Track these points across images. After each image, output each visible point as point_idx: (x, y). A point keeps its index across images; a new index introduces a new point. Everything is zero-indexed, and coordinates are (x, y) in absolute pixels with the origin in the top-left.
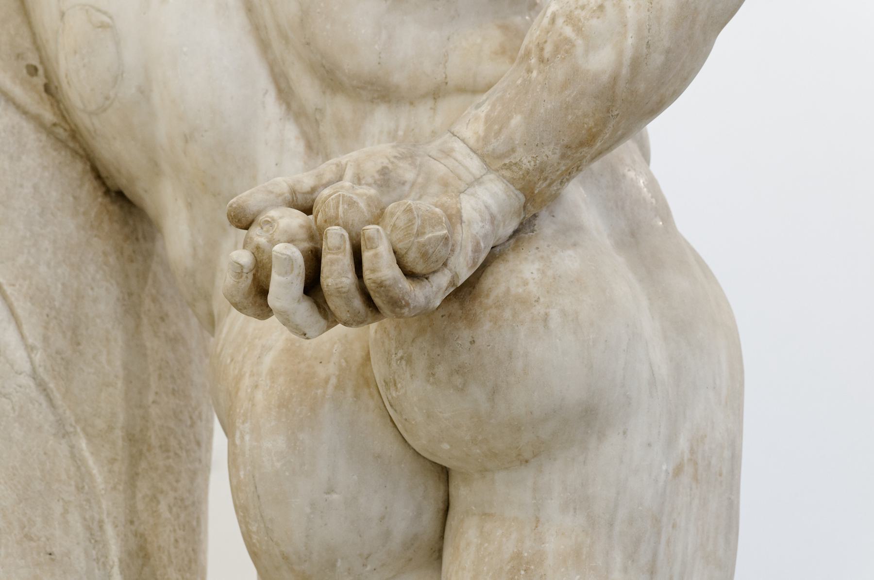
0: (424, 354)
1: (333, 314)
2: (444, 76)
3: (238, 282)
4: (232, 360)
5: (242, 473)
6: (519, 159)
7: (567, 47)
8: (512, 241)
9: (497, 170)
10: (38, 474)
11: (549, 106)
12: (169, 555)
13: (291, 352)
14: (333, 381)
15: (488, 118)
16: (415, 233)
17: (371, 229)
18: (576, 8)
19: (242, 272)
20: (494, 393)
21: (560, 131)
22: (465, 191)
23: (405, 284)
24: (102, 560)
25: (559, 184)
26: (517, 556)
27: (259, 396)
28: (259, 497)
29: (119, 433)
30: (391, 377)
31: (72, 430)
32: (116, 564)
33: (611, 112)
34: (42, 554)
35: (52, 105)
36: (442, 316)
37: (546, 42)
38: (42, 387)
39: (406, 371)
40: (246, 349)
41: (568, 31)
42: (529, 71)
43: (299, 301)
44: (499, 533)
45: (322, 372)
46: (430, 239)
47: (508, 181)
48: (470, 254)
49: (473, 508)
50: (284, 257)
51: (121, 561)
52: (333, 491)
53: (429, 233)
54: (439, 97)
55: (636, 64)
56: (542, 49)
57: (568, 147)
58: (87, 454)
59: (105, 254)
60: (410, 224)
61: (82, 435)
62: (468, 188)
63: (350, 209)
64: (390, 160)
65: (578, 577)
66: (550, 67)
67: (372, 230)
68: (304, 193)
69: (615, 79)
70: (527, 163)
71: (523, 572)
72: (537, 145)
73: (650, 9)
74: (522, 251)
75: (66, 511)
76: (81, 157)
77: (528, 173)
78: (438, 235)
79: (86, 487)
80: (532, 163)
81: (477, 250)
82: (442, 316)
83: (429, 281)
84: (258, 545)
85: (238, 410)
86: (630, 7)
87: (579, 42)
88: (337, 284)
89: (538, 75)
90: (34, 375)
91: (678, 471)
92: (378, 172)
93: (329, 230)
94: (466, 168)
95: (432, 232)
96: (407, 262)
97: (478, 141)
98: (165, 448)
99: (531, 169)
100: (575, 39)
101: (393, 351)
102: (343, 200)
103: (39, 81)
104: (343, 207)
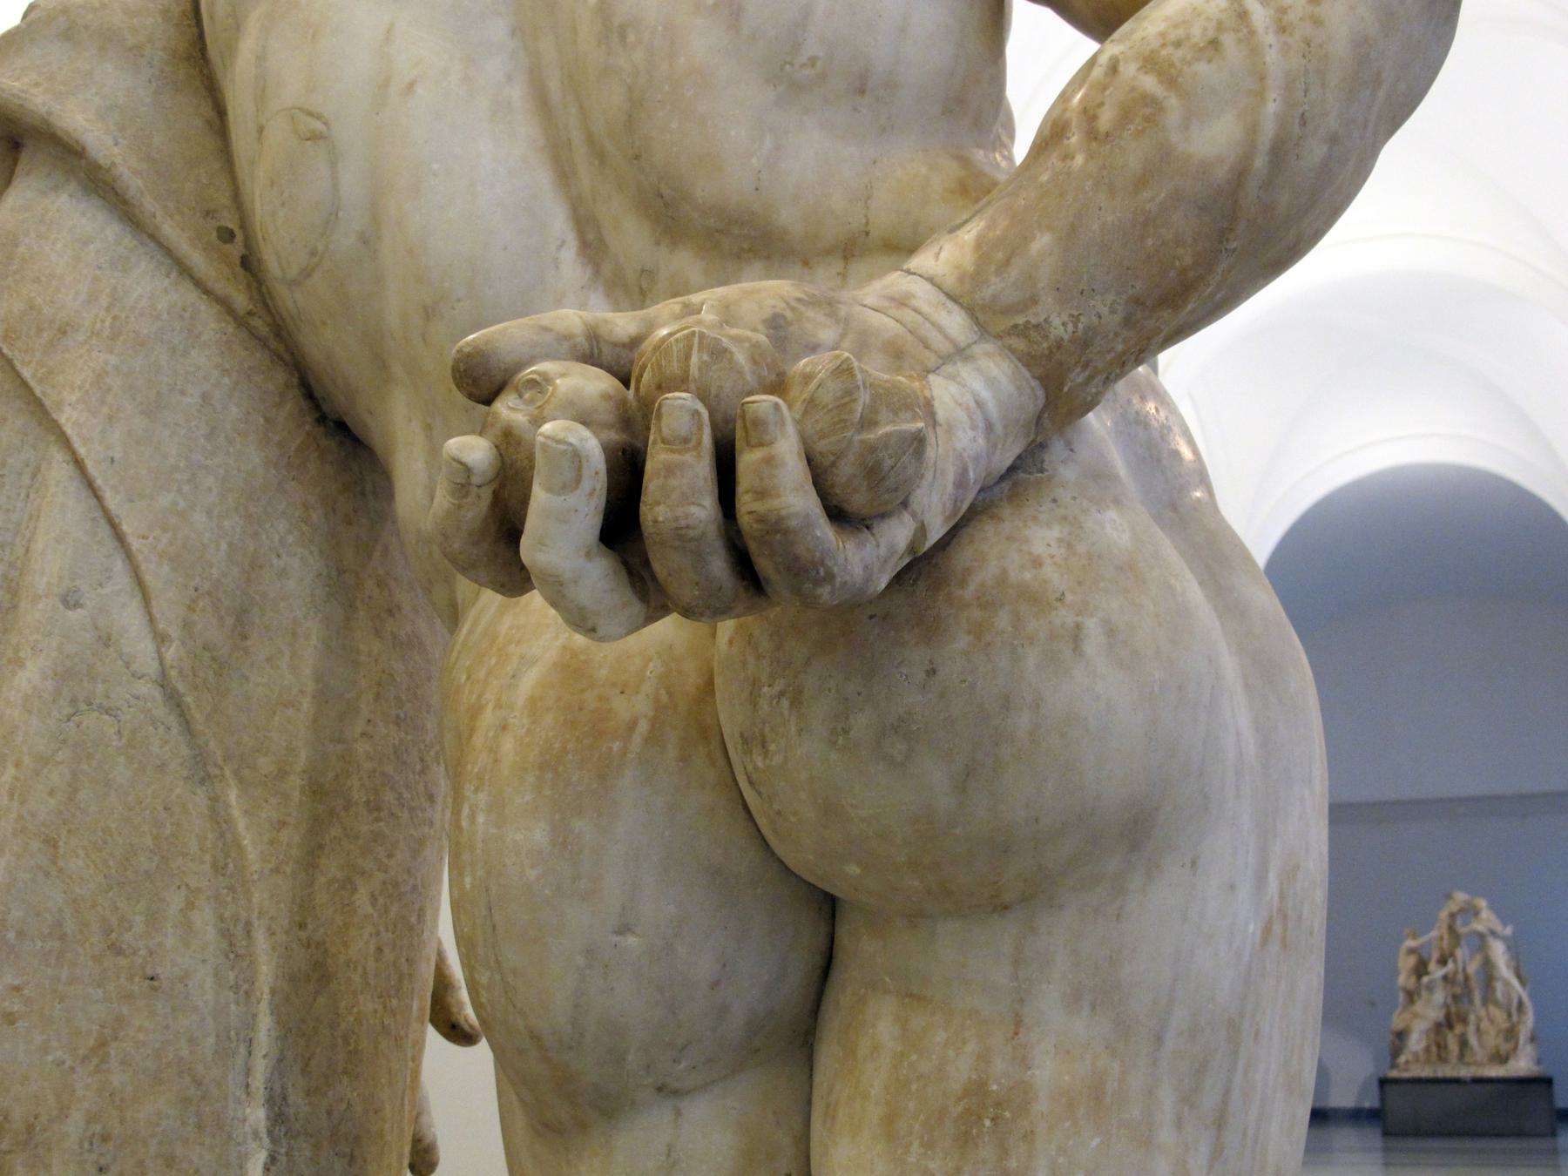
0: (830, 690)
1: (661, 590)
2: (864, 221)
3: (460, 507)
4: (468, 678)
5: (468, 880)
6: (1044, 317)
7: (1147, 111)
8: (1005, 485)
9: (999, 337)
10: (149, 841)
11: (1110, 219)
12: (365, 975)
13: (572, 671)
14: (643, 727)
15: (979, 243)
16: (857, 420)
17: (763, 402)
18: (1164, 45)
19: (470, 484)
20: (968, 775)
21: (1128, 269)
22: (938, 368)
23: (825, 531)
24: (246, 987)
25: (1101, 384)
26: (978, 1088)
27: (508, 745)
28: (494, 927)
29: (295, 782)
30: (756, 730)
31: (217, 772)
32: (265, 996)
33: (1225, 243)
34: (137, 979)
35: (249, 286)
36: (871, 617)
37: (1101, 104)
38: (174, 699)
39: (789, 721)
40: (493, 661)
41: (1150, 83)
42: (1068, 157)
43: (588, 554)
44: (941, 1036)
45: (622, 708)
46: (888, 435)
47: (1020, 360)
48: (950, 488)
49: (887, 979)
50: (563, 447)
51: (273, 992)
52: (629, 930)
53: (887, 424)
54: (853, 256)
55: (1280, 152)
56: (1094, 118)
57: (1137, 301)
58: (236, 812)
59: (306, 507)
60: (847, 400)
61: (232, 782)
62: (943, 364)
63: (715, 364)
64: (788, 304)
65: (1096, 1141)
66: (1112, 146)
67: (764, 404)
68: (615, 345)
69: (1240, 175)
70: (1060, 327)
71: (987, 1123)
72: (1082, 293)
73: (1307, 53)
74: (1027, 503)
75: (190, 905)
76: (286, 364)
77: (1059, 347)
78: (905, 431)
79: (231, 865)
80: (1070, 328)
81: (961, 483)
82: (871, 617)
83: (873, 535)
84: (489, 1009)
85: (469, 767)
86: (1271, 46)
87: (1173, 101)
88: (676, 519)
89: (1087, 161)
90: (163, 682)
91: (1267, 930)
92: (765, 321)
93: (667, 398)
94: (939, 328)
95: (893, 422)
96: (832, 486)
97: (961, 279)
98: (374, 806)
99: (1066, 337)
100: (1165, 98)
101: (764, 679)
102: (700, 343)
103: (236, 250)
104: (700, 358)
